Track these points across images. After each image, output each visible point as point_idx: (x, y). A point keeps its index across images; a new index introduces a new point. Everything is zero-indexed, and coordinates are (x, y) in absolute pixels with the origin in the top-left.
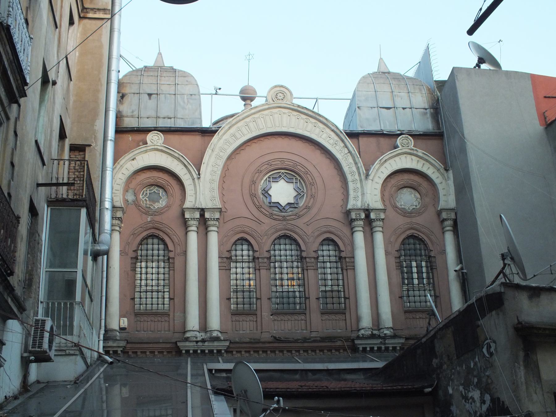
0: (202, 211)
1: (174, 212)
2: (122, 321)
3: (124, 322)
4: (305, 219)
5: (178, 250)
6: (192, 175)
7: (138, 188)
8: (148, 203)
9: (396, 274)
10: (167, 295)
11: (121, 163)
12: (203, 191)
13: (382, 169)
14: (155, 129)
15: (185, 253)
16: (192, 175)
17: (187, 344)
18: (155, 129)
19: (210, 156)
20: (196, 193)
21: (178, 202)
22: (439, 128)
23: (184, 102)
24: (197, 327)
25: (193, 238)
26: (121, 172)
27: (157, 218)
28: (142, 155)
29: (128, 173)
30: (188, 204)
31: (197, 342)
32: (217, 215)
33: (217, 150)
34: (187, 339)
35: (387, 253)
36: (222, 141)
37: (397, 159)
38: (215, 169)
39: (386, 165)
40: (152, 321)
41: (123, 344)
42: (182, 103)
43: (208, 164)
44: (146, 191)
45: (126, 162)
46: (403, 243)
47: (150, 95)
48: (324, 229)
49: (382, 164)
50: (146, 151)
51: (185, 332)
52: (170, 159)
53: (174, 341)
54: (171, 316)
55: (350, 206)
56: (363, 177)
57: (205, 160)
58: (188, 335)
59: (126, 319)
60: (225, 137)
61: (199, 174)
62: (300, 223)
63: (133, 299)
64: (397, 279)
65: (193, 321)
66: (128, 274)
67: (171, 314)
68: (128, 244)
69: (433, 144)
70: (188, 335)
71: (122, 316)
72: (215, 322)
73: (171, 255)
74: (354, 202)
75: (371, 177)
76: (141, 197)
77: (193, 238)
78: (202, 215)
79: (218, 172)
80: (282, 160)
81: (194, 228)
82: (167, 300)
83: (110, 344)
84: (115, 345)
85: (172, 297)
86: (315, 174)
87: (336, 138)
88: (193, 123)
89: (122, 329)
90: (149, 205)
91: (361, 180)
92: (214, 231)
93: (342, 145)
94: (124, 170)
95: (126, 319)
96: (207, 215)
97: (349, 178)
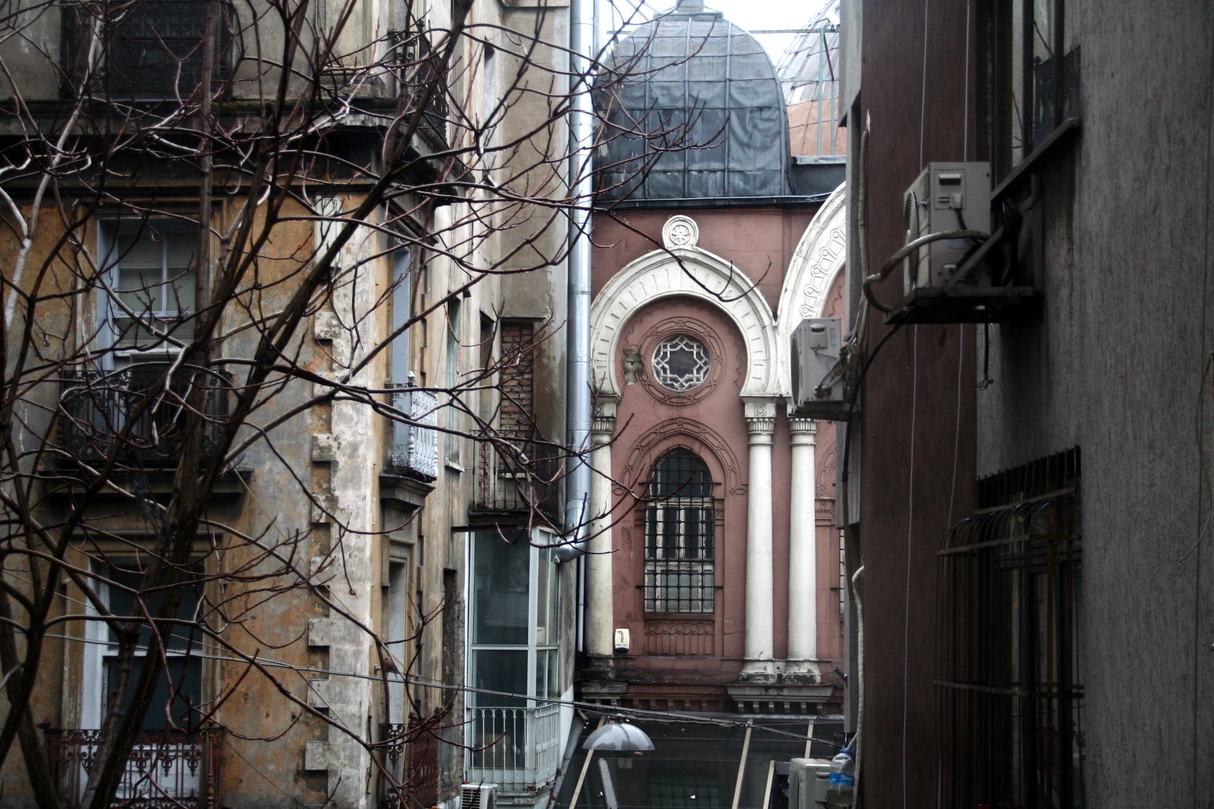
2: (618, 636)
3: (624, 638)
5: (733, 483)
6: (760, 319)
7: (646, 344)
8: (669, 375)
11: (609, 294)
15: (745, 489)
16: (760, 319)
19: (800, 272)
20: (768, 360)
24: (768, 653)
25: (762, 460)
26: (609, 313)
27: (687, 413)
28: (653, 272)
29: (624, 315)
30: (751, 387)
31: (767, 688)
33: (815, 256)
36: (826, 233)
38: (811, 301)
40: (678, 633)
42: (739, 131)
43: (794, 291)
44: (665, 347)
45: (619, 291)
51: (744, 662)
53: (720, 678)
54: (718, 625)
57: (789, 282)
58: (750, 670)
59: (626, 632)
61: (775, 317)
63: (640, 587)
65: (761, 640)
66: (629, 534)
67: (718, 619)
68: (628, 469)
70: (750, 670)
71: (618, 624)
72: (805, 642)
76: (654, 361)
77: (762, 460)
79: (816, 309)
81: (765, 439)
84: (605, 690)
85: (718, 584)
89: (620, 653)
90: (672, 379)
92: (806, 445)
94: (615, 308)
95: (626, 632)
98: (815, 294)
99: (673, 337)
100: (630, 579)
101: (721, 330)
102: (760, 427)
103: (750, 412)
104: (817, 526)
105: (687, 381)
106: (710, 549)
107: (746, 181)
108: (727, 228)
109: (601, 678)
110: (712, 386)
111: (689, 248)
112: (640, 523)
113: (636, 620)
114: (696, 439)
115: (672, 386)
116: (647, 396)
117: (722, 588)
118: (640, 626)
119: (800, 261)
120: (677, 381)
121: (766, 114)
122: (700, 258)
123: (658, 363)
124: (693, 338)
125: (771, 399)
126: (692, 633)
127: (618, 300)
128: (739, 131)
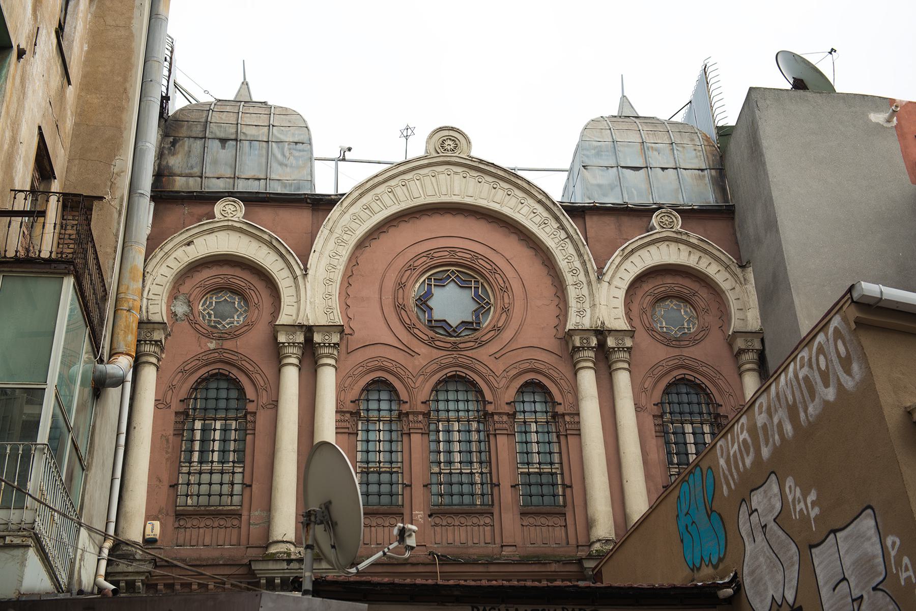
0: (309, 330)
1: (259, 334)
2: (149, 527)
3: (155, 529)
4: (493, 348)
5: (264, 399)
6: (292, 271)
7: (195, 292)
8: (213, 318)
9: (654, 443)
10: (238, 478)
11: (166, 249)
12: (312, 298)
13: (627, 265)
14: (231, 194)
15: (275, 404)
16: (292, 271)
17: (271, 566)
18: (231, 194)
20: (298, 301)
21: (266, 317)
22: (725, 199)
23: (284, 155)
24: (291, 536)
25: (291, 377)
26: (164, 265)
27: (228, 345)
28: (205, 237)
29: (177, 267)
30: (283, 319)
32: (335, 338)
33: (338, 231)
34: (274, 558)
35: (638, 408)
36: (347, 216)
37: (653, 249)
38: (335, 262)
39: (634, 258)
40: (207, 526)
41: (147, 567)
42: (279, 156)
43: (321, 253)
44: (211, 298)
45: (175, 248)
46: (666, 392)
47: (223, 141)
48: (526, 366)
49: (626, 258)
50: (212, 231)
52: (255, 244)
53: (246, 561)
54: (244, 518)
55: (570, 326)
56: (593, 277)
57: (318, 244)
58: (273, 550)
59: (157, 524)
60: (353, 210)
61: (306, 269)
62: (483, 354)
63: (174, 486)
64: (657, 454)
66: (167, 440)
67: (245, 513)
68: (172, 387)
69: (718, 226)
70: (273, 550)
71: (149, 517)
73: (251, 407)
74: (579, 318)
75: (607, 278)
76: (200, 307)
77: (291, 377)
78: (309, 340)
79: (338, 267)
80: (452, 250)
81: (294, 361)
82: (237, 489)
83: (122, 567)
84: (130, 569)
85: (247, 482)
86: (510, 274)
87: (545, 214)
88: (299, 189)
89: (149, 542)
90: (215, 322)
91: (589, 283)
92: (329, 365)
93: (556, 225)
94: (171, 261)
95: (157, 524)
96: (317, 338)
97: (569, 279)
98: (338, 257)
99: (218, 289)
100: (165, 477)
101: (259, 285)
102: (291, 350)
103: (282, 338)
104: (337, 433)
105: (228, 324)
106: (240, 451)
107: (285, 186)
108: (266, 214)
109: (130, 558)
110: (249, 325)
111: (237, 219)
112: (179, 433)
113: (167, 514)
114: (234, 366)
115: (215, 327)
116: (192, 331)
117: (250, 486)
118: (171, 519)
119: (326, 232)
120: (219, 323)
121: (300, 146)
122: (245, 227)
123: (204, 310)
124: (235, 291)
125: (301, 326)
126: (220, 527)
127: (174, 255)
128: (279, 156)
